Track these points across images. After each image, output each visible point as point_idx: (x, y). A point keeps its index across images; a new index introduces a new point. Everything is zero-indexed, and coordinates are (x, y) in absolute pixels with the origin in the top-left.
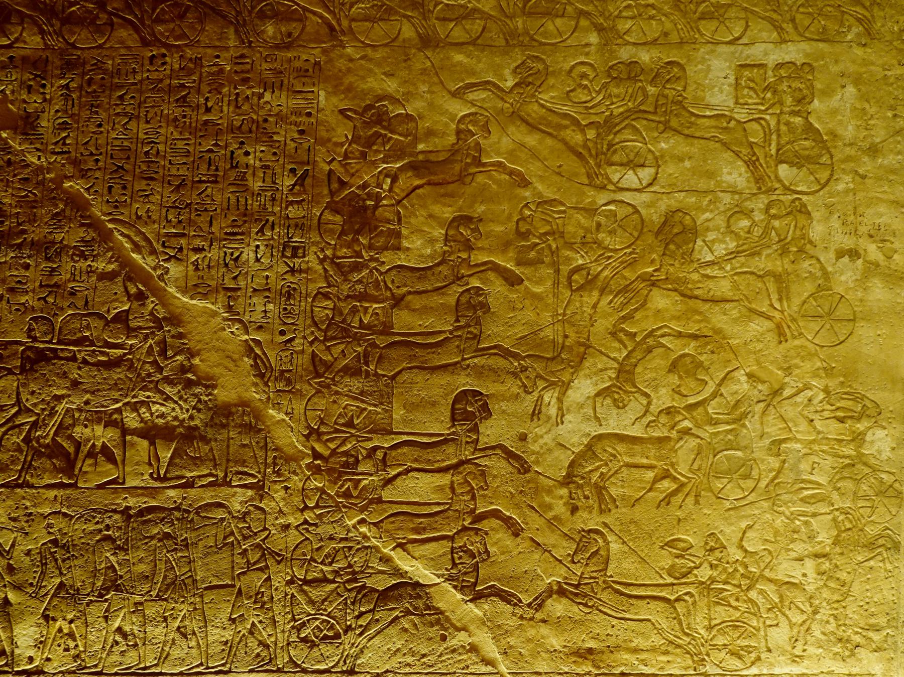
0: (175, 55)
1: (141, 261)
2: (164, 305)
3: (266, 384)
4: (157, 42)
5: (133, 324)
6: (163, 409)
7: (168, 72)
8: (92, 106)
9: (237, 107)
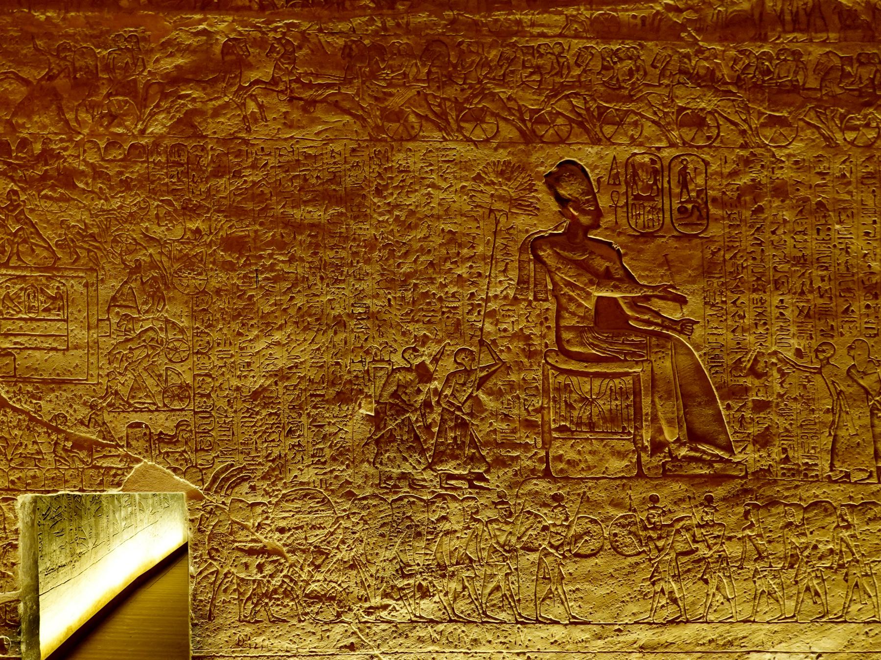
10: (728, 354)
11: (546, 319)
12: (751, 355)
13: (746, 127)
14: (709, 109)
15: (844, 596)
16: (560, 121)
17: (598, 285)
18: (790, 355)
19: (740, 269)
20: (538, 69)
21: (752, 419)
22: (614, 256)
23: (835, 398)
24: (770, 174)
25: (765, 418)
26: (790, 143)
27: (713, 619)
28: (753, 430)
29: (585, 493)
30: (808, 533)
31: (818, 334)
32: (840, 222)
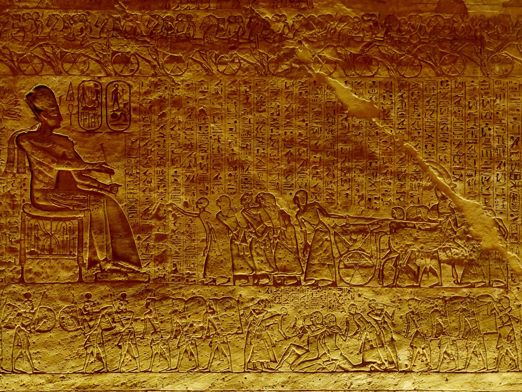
0: (453, 81)
1: (443, 181)
2: (455, 202)
3: (506, 240)
4: (443, 74)
5: (441, 211)
6: (457, 251)
7: (450, 89)
8: (415, 106)
9: (483, 106)
10: (140, 206)
11: (24, 185)
12: (156, 206)
13: (156, 63)
14: (132, 52)
16: (36, 61)
17: (58, 163)
18: (180, 205)
19: (149, 152)
20: (22, 29)
21: (154, 246)
22: (70, 144)
23: (208, 232)
24: (171, 93)
25: (162, 245)
26: (184, 73)
28: (154, 253)
29: (45, 292)
30: (187, 317)
31: (198, 192)
32: (214, 122)
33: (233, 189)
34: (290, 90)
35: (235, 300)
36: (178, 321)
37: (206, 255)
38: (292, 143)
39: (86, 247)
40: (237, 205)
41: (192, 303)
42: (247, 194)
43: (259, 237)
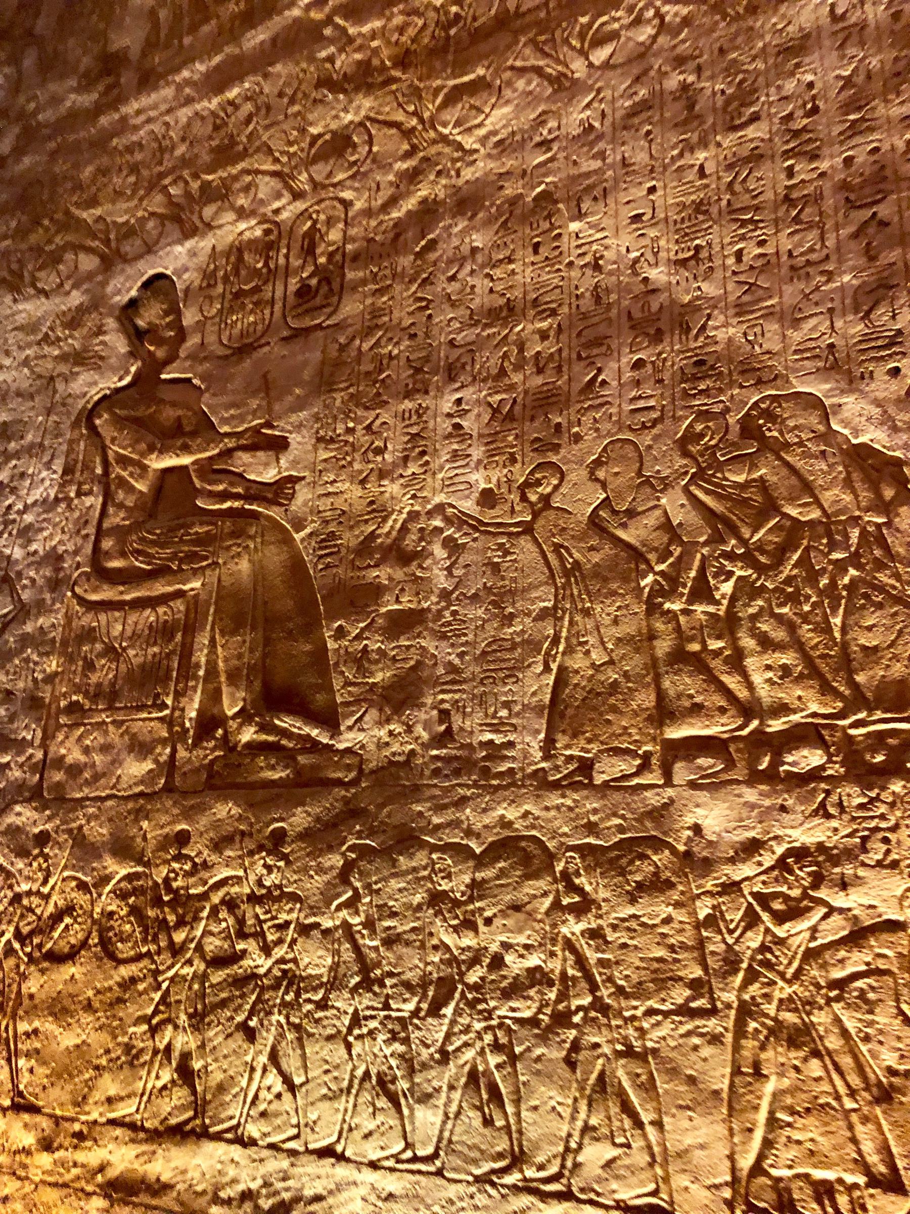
10: (351, 528)
12: (396, 521)
13: (414, 122)
15: (566, 1112)
20: (134, 169)
25: (408, 648)
27: (256, 1135)
29: (80, 828)
30: (480, 922)
31: (527, 448)
32: (580, 216)
33: (652, 408)
34: (853, 20)
35: (674, 851)
36: (449, 939)
37: (554, 667)
38: (881, 186)
39: (196, 677)
40: (667, 463)
41: (502, 864)
42: (703, 415)
43: (761, 569)
